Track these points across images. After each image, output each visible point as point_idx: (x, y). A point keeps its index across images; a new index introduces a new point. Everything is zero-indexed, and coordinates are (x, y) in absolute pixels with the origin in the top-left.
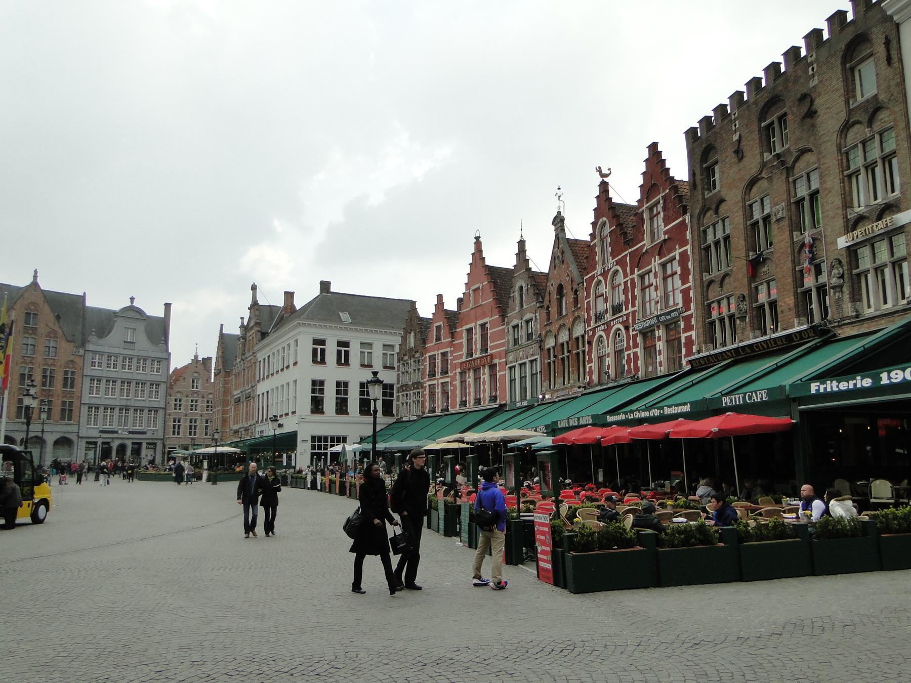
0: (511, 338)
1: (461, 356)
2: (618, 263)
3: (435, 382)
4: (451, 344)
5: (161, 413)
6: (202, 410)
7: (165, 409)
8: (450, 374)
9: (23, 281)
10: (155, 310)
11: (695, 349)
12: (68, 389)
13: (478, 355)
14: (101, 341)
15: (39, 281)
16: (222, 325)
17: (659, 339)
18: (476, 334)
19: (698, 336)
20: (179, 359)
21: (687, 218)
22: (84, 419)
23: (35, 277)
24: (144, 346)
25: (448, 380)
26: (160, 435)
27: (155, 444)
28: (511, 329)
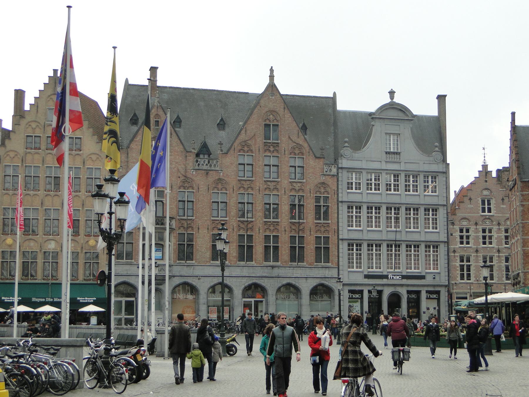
5: (442, 249)
6: (499, 243)
7: (447, 243)
9: (258, 87)
10: (424, 107)
12: (322, 221)
14: (356, 155)
15: (276, 82)
16: (513, 114)
20: (462, 174)
22: (344, 261)
23: (272, 77)
24: (413, 157)
26: (444, 281)
27: (438, 293)
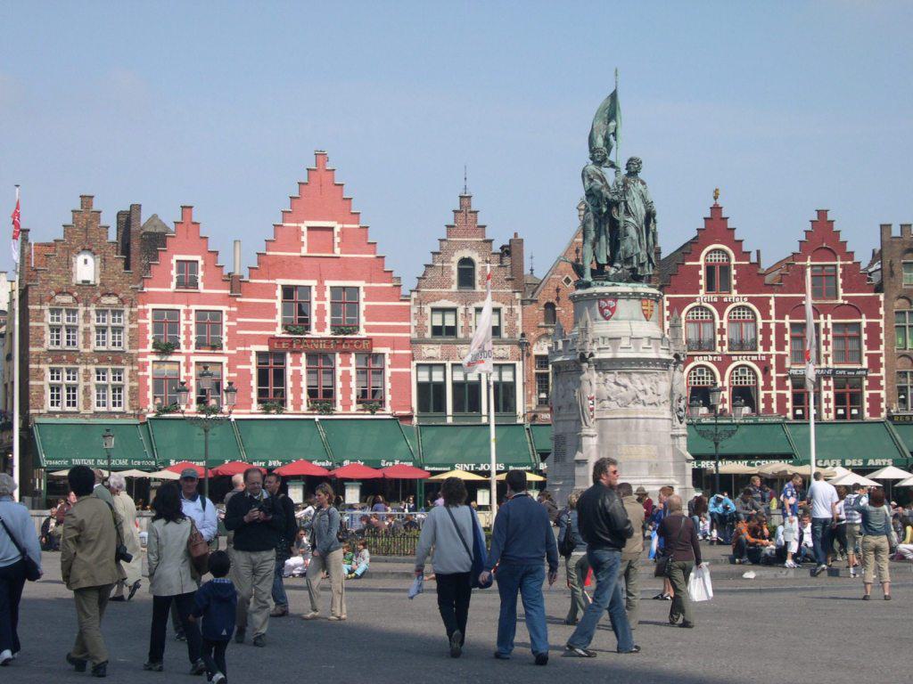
0: (428, 323)
1: (273, 326)
2: (750, 300)
3: (182, 359)
4: (229, 300)
8: (226, 350)
11: (883, 405)
13: (328, 333)
17: (827, 388)
18: (321, 297)
19: (888, 396)
21: (882, 297)
25: (225, 360)
28: (427, 309)
